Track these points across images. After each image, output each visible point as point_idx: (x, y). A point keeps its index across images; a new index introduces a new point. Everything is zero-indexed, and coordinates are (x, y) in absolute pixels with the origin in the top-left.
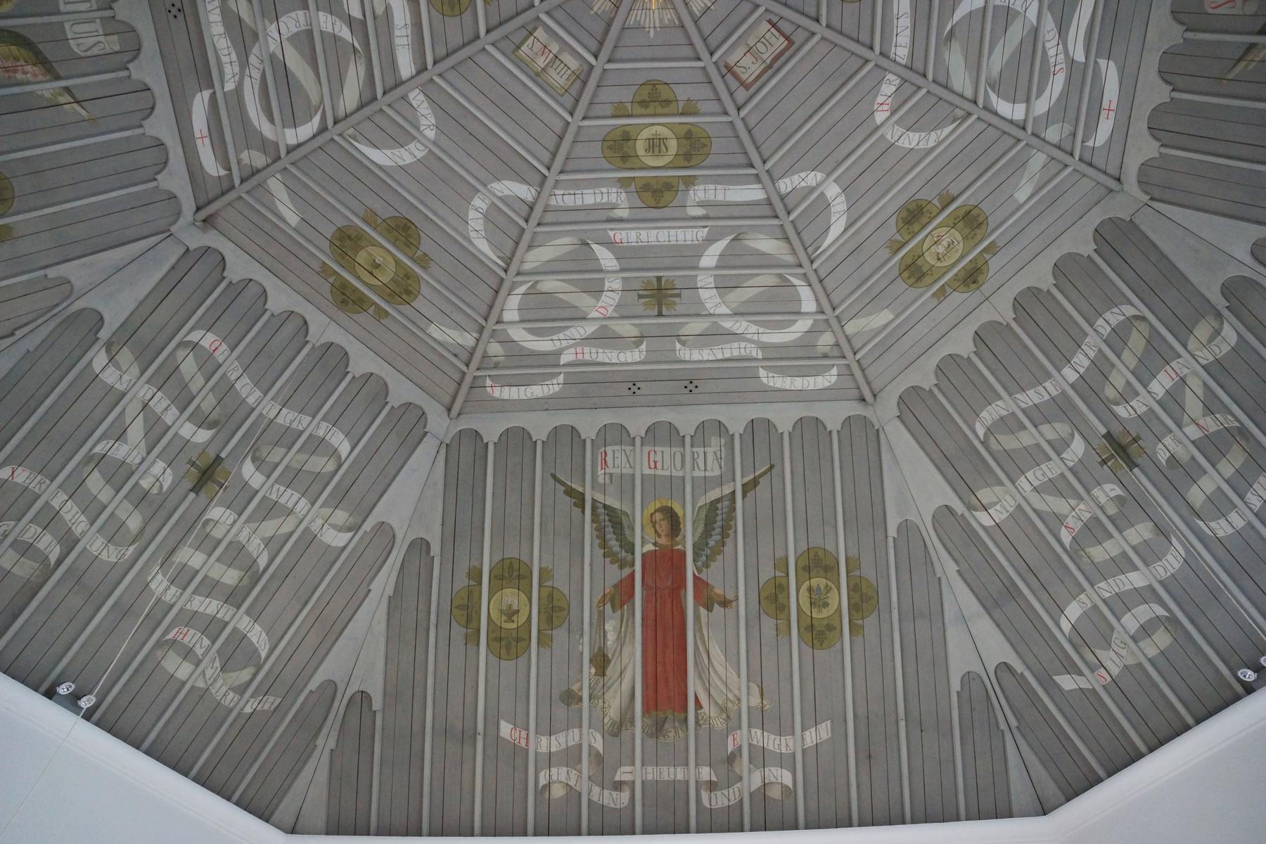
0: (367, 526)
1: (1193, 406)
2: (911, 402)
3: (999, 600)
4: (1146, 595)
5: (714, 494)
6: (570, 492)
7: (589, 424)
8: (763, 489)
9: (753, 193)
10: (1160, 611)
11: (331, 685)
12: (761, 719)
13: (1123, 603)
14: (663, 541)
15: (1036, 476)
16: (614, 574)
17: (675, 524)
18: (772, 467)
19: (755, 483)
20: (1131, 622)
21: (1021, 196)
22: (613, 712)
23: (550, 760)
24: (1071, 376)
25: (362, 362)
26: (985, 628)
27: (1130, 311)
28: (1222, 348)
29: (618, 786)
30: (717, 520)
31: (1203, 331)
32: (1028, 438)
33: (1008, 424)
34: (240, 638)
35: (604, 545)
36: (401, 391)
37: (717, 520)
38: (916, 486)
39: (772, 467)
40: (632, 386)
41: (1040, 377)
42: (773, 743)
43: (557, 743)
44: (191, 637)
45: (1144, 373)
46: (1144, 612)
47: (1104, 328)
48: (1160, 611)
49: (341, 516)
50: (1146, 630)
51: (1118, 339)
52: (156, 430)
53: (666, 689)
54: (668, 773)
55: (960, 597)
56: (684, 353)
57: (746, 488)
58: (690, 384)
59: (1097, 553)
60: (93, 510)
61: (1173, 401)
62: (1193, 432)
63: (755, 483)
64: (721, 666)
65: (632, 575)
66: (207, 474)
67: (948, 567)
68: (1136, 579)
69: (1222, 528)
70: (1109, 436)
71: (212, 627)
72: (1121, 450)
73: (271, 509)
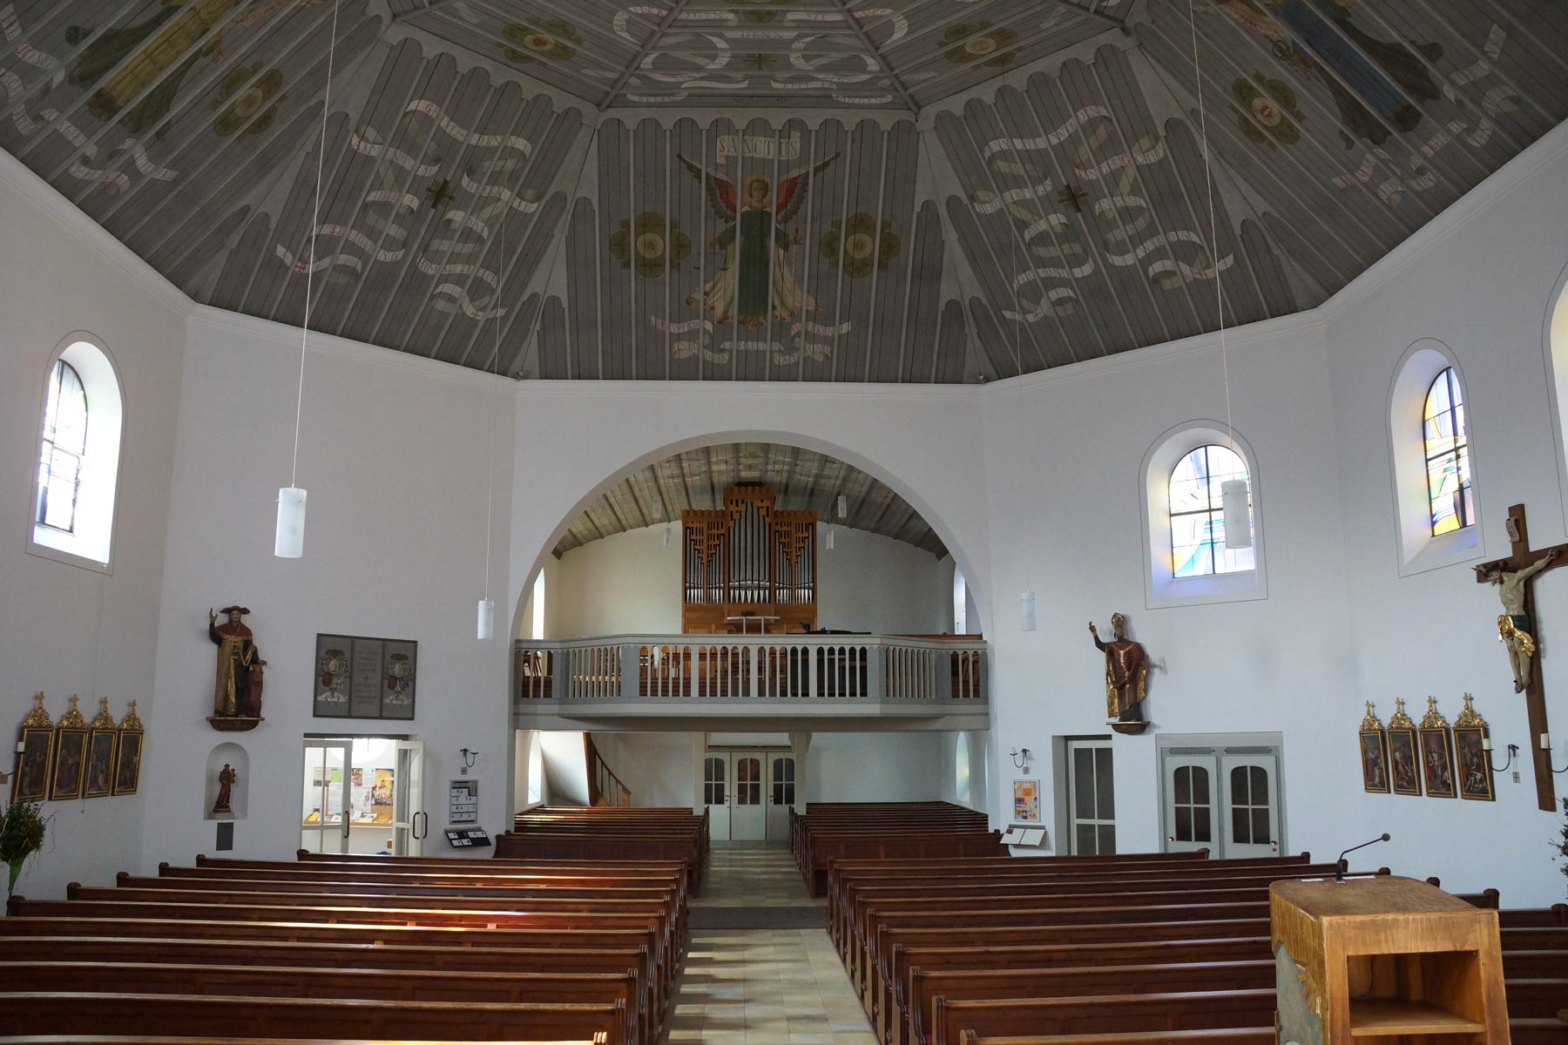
0: (548, 197)
1: (1125, 185)
2: (944, 119)
3: (976, 258)
4: (1064, 283)
5: (795, 173)
6: (690, 167)
7: (704, 118)
8: (829, 171)
9: (838, 17)
10: (1072, 294)
11: (535, 296)
12: (813, 317)
13: (1051, 283)
14: (757, 205)
15: (1014, 194)
16: (721, 226)
17: (765, 188)
18: (838, 155)
19: (825, 165)
20: (1053, 295)
21: (1045, 26)
22: (719, 312)
23: (678, 337)
24: (1054, 141)
25: (531, 89)
26: (966, 271)
27: (1104, 113)
28: (1152, 158)
29: (723, 351)
30: (793, 190)
31: (1145, 142)
32: (1017, 168)
33: (1004, 155)
34: (479, 282)
35: (714, 206)
36: (561, 102)
37: (793, 190)
38: (937, 178)
39: (838, 155)
40: (738, 100)
41: (1034, 135)
42: (820, 329)
43: (684, 328)
44: (446, 288)
45: (1102, 153)
46: (1063, 292)
47: (1082, 116)
48: (1072, 294)
49: (530, 193)
50: (1061, 301)
51: (1091, 126)
52: (400, 174)
53: (754, 295)
54: (751, 346)
55: (954, 249)
56: (775, 85)
57: (817, 170)
58: (781, 100)
59: (1042, 252)
60: (372, 234)
61: (1114, 178)
62: (1119, 202)
63: (825, 165)
64: (789, 286)
65: (734, 227)
66: (440, 194)
67: (950, 235)
68: (1064, 273)
69: (1118, 261)
70: (1068, 186)
71: (460, 280)
72: (1074, 198)
73: (485, 202)
